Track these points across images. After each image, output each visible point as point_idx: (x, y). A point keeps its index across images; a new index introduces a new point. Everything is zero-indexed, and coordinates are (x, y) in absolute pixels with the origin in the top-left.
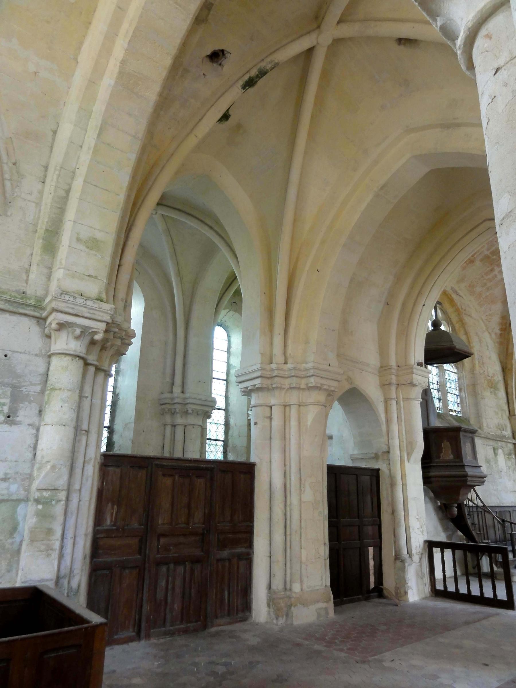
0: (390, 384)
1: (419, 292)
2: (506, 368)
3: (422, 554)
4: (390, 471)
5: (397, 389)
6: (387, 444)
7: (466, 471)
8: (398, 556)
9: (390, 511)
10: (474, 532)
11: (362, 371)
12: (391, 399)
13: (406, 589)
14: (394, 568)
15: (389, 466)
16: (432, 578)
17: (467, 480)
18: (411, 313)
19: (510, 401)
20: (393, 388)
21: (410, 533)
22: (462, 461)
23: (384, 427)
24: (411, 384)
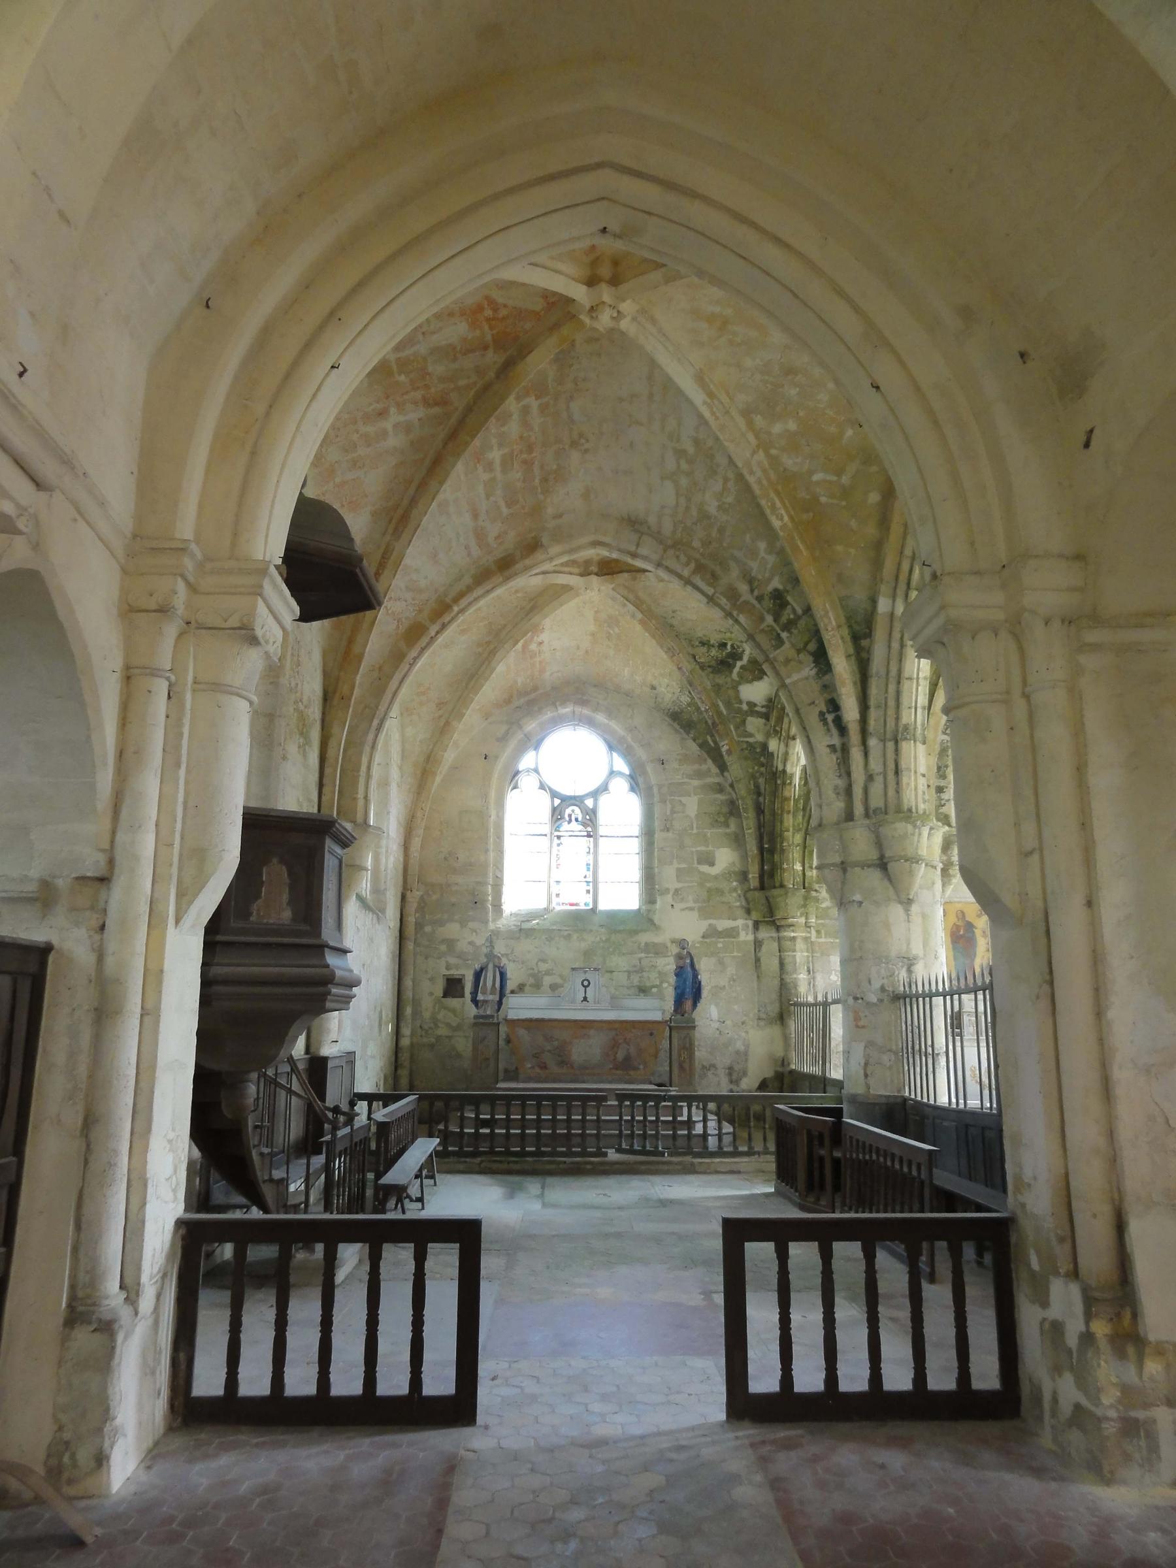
0: (164, 610)
1: (332, 314)
2: (335, 692)
3: (164, 1276)
4: (101, 959)
5: (181, 635)
6: (107, 846)
7: (328, 966)
8: (81, 1309)
9: (73, 1118)
10: (254, 1153)
11: (78, 517)
12: (154, 673)
13: (107, 1444)
14: (60, 1363)
15: (97, 937)
16: (182, 1356)
17: (329, 993)
18: (288, 376)
19: (325, 781)
20: (171, 631)
21: (144, 1204)
22: (319, 935)
23: (105, 780)
24: (243, 632)
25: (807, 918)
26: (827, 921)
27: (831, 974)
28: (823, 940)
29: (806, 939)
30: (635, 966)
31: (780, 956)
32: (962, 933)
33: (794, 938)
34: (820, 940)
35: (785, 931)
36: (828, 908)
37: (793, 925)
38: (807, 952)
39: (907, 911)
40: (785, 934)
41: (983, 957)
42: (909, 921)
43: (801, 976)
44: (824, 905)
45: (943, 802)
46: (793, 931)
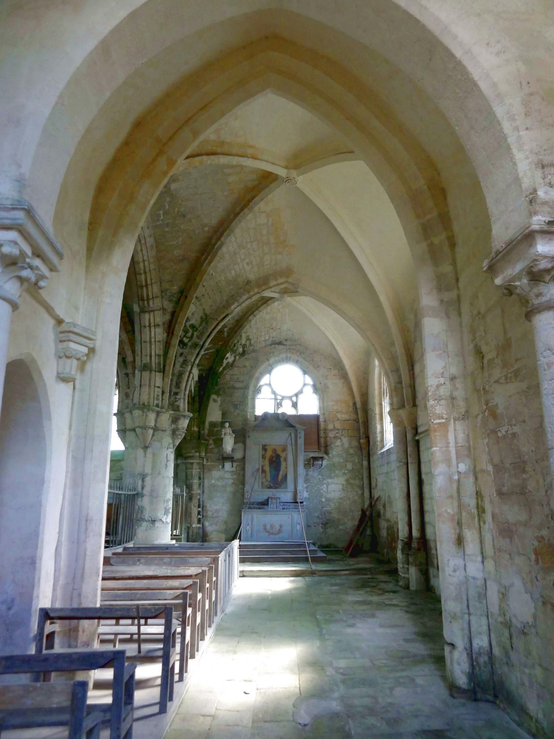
25: (200, 453)
26: (212, 454)
27: (212, 480)
28: (209, 463)
29: (199, 463)
30: (118, 477)
31: (186, 471)
32: (274, 459)
33: (192, 463)
34: (207, 464)
35: (188, 459)
36: (213, 448)
37: (192, 457)
38: (199, 469)
39: (145, 452)
40: (189, 461)
41: (284, 471)
42: (145, 457)
43: (195, 481)
44: (211, 447)
45: (177, 400)
46: (192, 459)
